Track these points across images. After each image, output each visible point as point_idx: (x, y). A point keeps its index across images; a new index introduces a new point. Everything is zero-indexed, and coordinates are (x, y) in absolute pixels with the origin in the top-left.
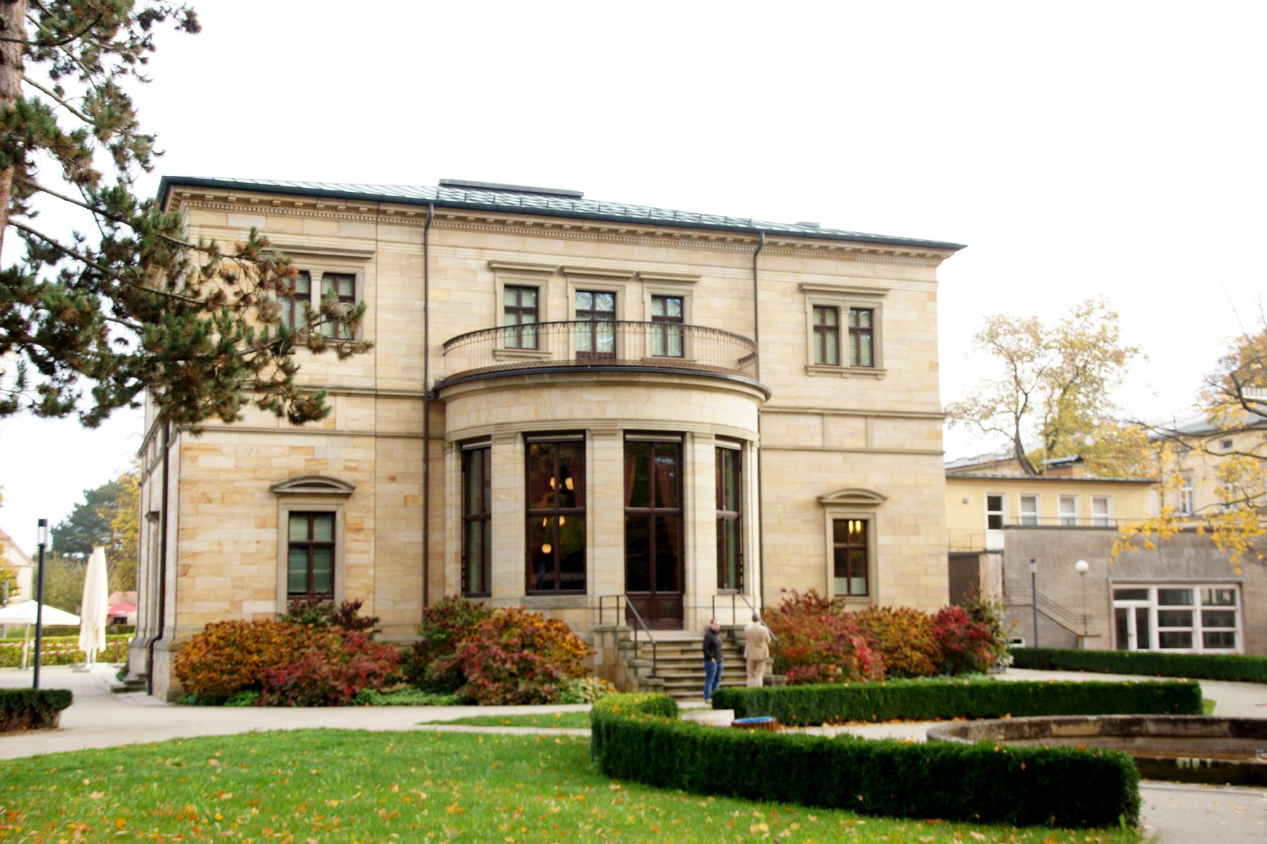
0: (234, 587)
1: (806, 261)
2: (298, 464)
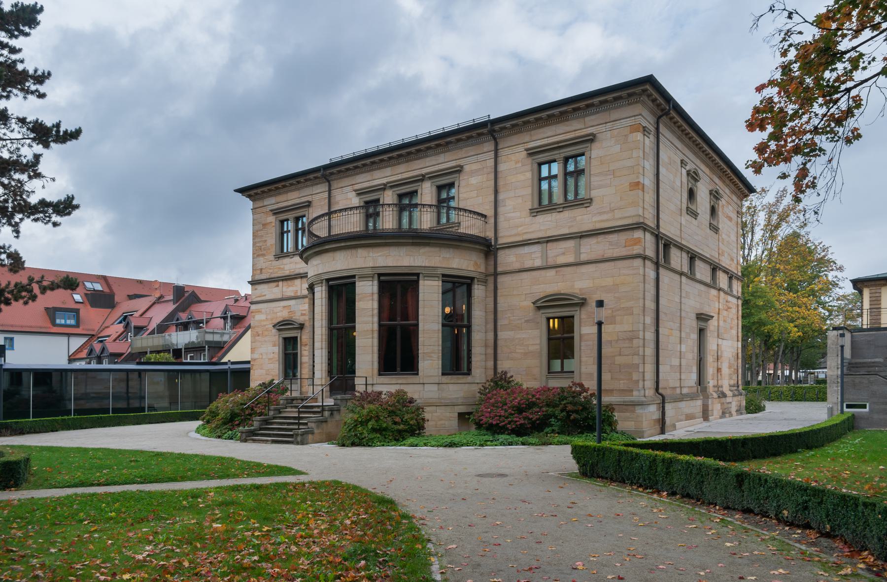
0: (267, 374)
1: (533, 132)
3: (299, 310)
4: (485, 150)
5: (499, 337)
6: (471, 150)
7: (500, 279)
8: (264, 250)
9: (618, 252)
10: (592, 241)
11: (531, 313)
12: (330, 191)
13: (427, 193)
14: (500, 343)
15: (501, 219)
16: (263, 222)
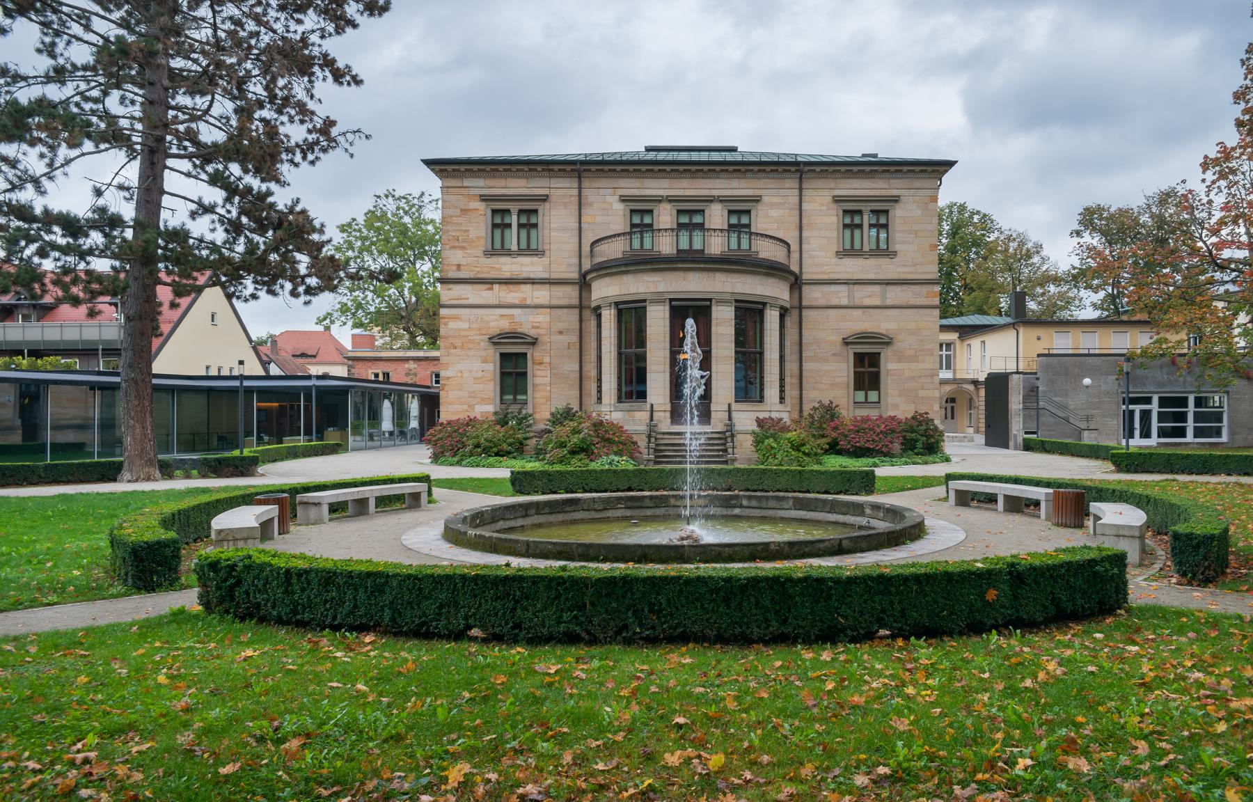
2: (504, 325)
3: (527, 322)
4: (787, 186)
5: (804, 367)
6: (771, 183)
7: (805, 313)
8: (464, 241)
9: (919, 302)
10: (897, 289)
11: (838, 347)
12: (580, 188)
13: (716, 216)
14: (804, 373)
15: (805, 255)
16: (463, 207)
